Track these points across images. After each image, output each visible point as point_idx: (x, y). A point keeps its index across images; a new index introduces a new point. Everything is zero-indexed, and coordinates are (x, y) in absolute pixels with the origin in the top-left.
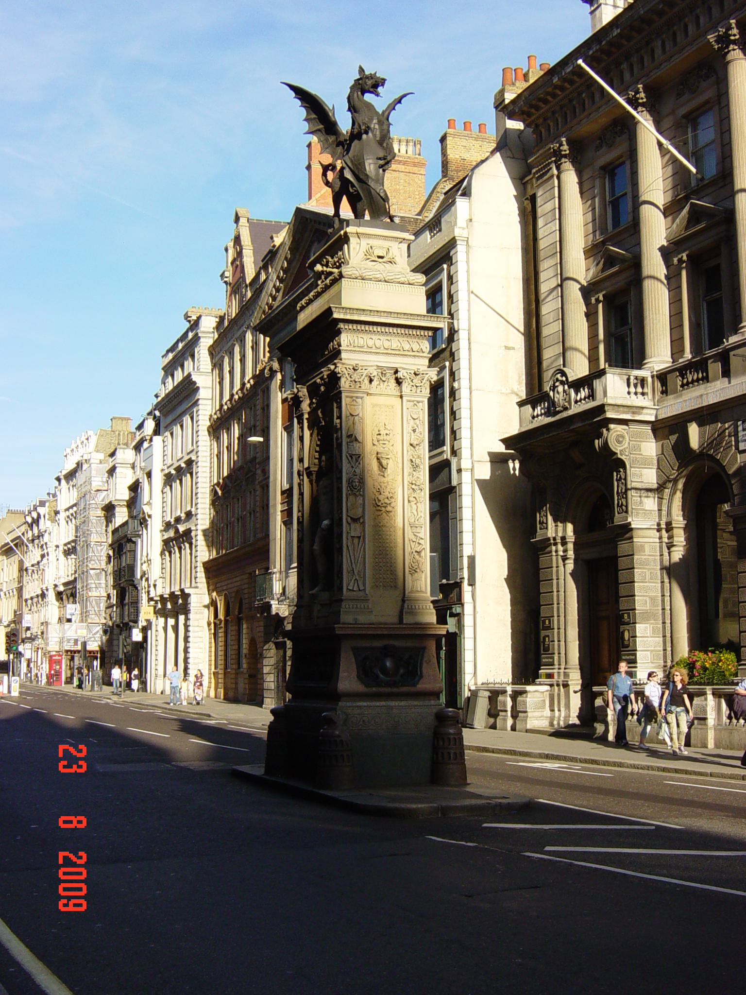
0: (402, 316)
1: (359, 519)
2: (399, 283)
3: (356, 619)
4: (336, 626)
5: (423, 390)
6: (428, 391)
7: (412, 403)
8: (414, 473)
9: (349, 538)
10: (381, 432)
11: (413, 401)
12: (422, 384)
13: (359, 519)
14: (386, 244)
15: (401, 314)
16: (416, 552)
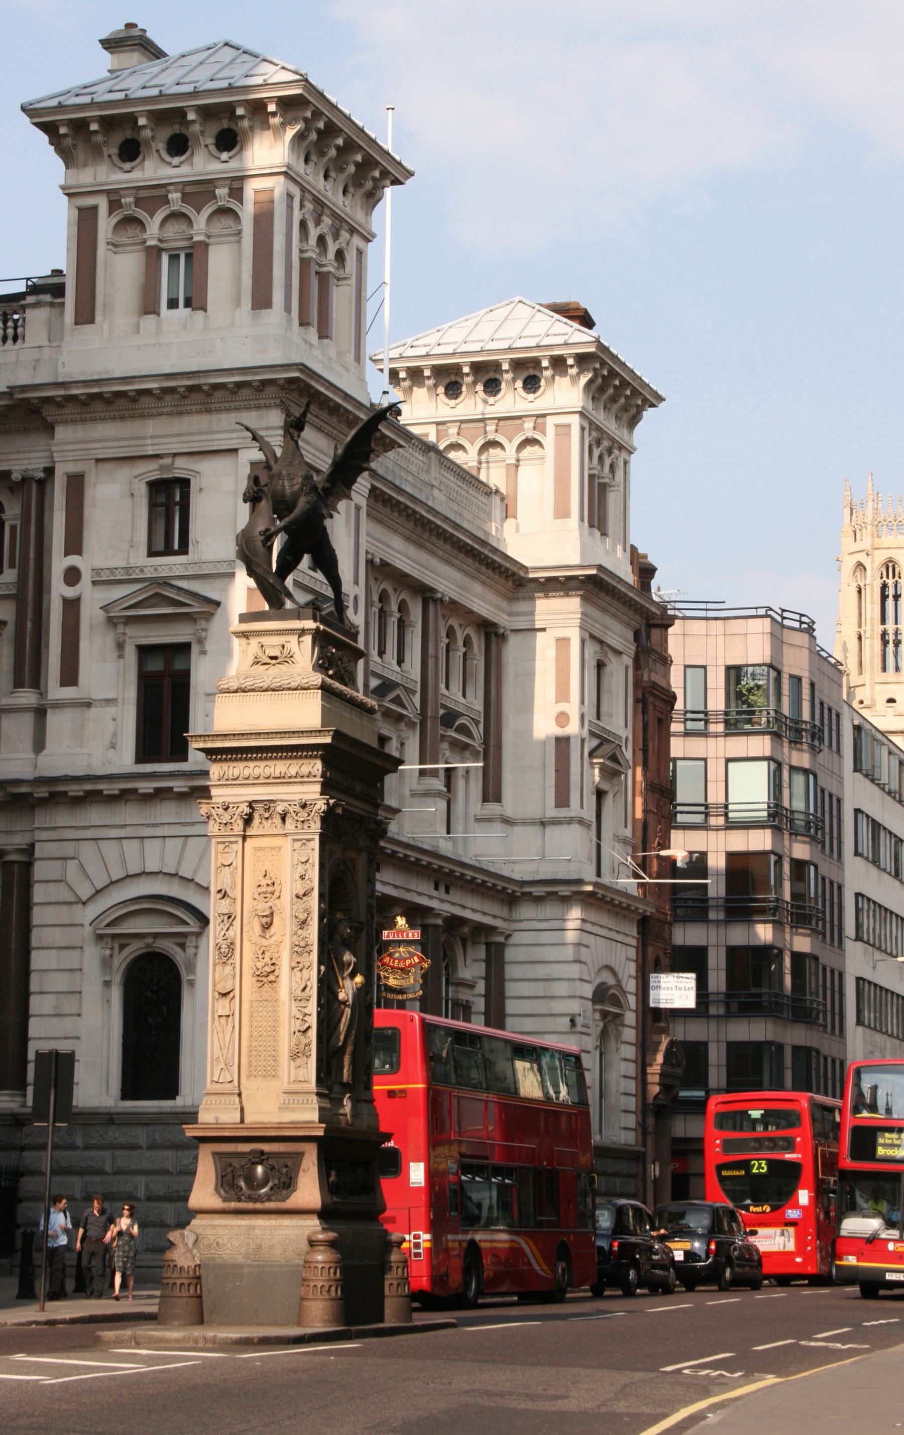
0: (274, 736)
1: (229, 993)
2: (290, 689)
3: (217, 1118)
4: (184, 1126)
5: (312, 824)
6: (319, 824)
7: (300, 843)
8: (300, 932)
9: (216, 1017)
10: (261, 883)
11: (301, 840)
12: (310, 818)
13: (229, 993)
14: (280, 640)
15: (272, 733)
16: (299, 1031)
